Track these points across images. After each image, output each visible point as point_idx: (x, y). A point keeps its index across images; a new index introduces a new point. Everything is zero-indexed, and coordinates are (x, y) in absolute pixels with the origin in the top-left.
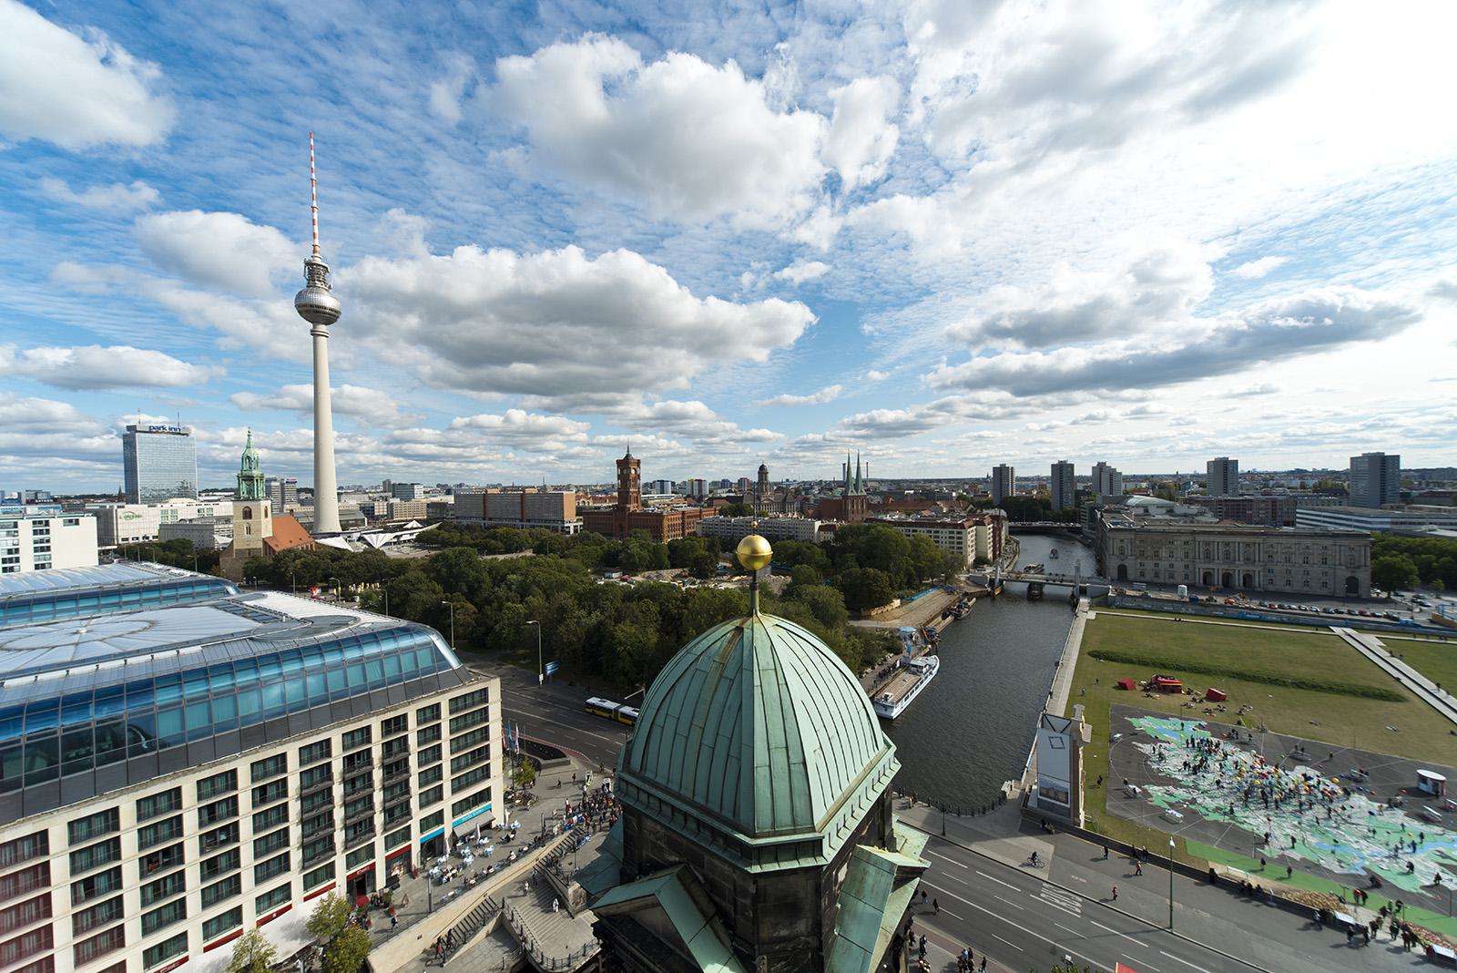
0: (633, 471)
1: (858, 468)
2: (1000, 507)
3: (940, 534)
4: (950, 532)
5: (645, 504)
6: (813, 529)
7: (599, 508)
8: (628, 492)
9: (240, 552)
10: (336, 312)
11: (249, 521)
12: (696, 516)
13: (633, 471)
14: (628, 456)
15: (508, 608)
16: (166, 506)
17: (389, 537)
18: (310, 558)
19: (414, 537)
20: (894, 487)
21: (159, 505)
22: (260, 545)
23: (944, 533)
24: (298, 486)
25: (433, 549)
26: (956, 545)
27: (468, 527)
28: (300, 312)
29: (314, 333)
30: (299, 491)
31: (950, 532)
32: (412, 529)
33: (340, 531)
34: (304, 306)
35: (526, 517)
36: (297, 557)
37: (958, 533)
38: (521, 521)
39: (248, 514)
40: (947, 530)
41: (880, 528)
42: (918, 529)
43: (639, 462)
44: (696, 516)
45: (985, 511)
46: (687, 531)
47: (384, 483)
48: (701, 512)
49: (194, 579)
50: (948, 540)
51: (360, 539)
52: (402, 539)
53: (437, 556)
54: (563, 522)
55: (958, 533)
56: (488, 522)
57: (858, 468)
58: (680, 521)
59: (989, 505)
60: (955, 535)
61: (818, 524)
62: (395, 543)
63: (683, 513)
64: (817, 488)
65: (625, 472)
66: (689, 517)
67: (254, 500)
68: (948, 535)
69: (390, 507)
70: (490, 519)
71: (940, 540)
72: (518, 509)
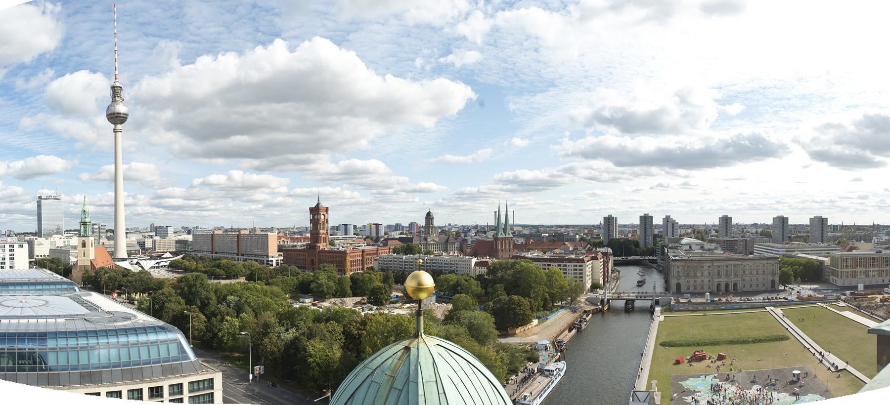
0: (322, 217)
1: (507, 215)
2: (608, 246)
3: (567, 268)
4: (574, 266)
5: (332, 243)
6: (470, 265)
7: (296, 246)
8: (318, 234)
9: (80, 267)
10: (126, 115)
11: (84, 249)
12: (373, 254)
13: (322, 217)
14: (318, 205)
15: (227, 321)
16: (52, 239)
17: (153, 263)
18: (112, 274)
19: (168, 264)
20: (534, 231)
21: (49, 239)
22: (89, 264)
23: (570, 266)
24: (107, 228)
25: (179, 273)
26: (578, 276)
27: (201, 258)
28: (108, 119)
29: (115, 131)
30: (107, 231)
31: (574, 266)
32: (167, 258)
33: (127, 258)
34: (111, 114)
35: (241, 252)
36: (106, 272)
37: (580, 266)
38: (238, 255)
39: (84, 245)
40: (572, 264)
41: (523, 263)
42: (552, 264)
43: (327, 210)
44: (373, 254)
45: (598, 249)
46: (366, 266)
47: (151, 225)
48: (377, 250)
49: (62, 280)
50: (573, 272)
51: (138, 263)
52: (161, 265)
53: (182, 278)
54: (268, 256)
55: (580, 266)
56: (215, 255)
57: (507, 215)
58: (361, 258)
59: (600, 244)
60: (578, 268)
61: (474, 260)
62: (156, 267)
63: (363, 251)
64: (473, 231)
65: (316, 217)
66: (367, 254)
67: (86, 236)
68: (573, 268)
69: (154, 242)
70: (216, 253)
71: (567, 271)
72: (235, 245)
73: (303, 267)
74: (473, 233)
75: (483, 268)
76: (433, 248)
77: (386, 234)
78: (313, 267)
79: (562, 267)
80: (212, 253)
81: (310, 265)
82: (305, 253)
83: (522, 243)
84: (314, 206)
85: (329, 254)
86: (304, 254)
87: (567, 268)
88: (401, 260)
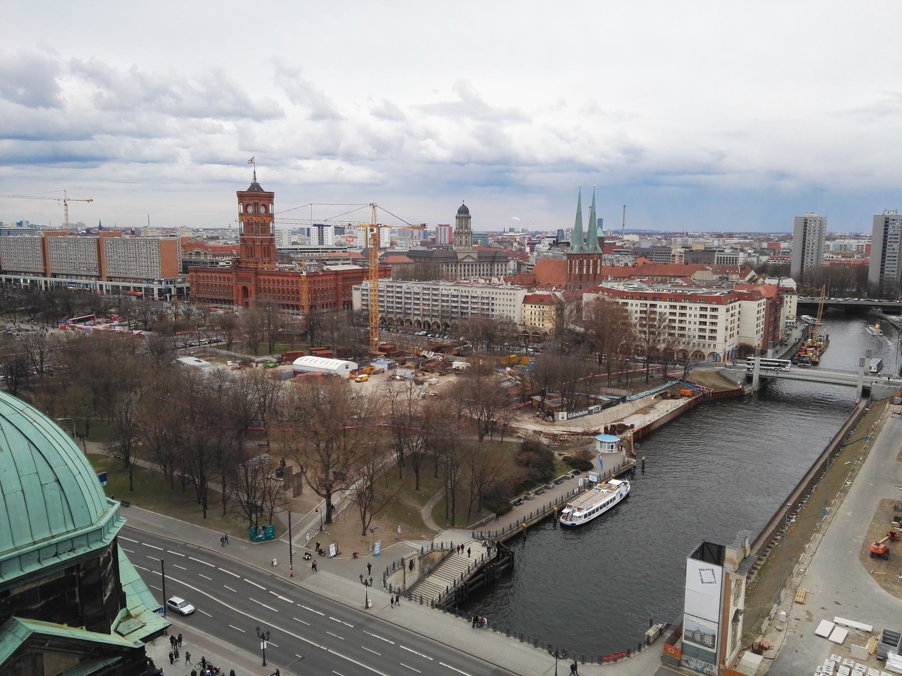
0: (262, 210)
13: (262, 210)
43: (270, 197)
63: (336, 273)
73: (228, 301)
74: (543, 247)
75: (537, 306)
76: (468, 270)
77: (392, 244)
78: (246, 300)
79: (678, 311)
80: (45, 275)
81: (240, 298)
82: (231, 276)
83: (626, 264)
84: (245, 188)
85: (276, 278)
86: (228, 277)
87: (688, 312)
88: (399, 290)
